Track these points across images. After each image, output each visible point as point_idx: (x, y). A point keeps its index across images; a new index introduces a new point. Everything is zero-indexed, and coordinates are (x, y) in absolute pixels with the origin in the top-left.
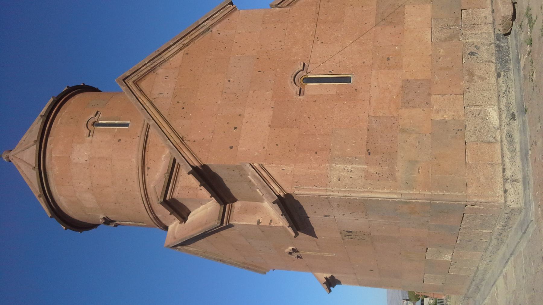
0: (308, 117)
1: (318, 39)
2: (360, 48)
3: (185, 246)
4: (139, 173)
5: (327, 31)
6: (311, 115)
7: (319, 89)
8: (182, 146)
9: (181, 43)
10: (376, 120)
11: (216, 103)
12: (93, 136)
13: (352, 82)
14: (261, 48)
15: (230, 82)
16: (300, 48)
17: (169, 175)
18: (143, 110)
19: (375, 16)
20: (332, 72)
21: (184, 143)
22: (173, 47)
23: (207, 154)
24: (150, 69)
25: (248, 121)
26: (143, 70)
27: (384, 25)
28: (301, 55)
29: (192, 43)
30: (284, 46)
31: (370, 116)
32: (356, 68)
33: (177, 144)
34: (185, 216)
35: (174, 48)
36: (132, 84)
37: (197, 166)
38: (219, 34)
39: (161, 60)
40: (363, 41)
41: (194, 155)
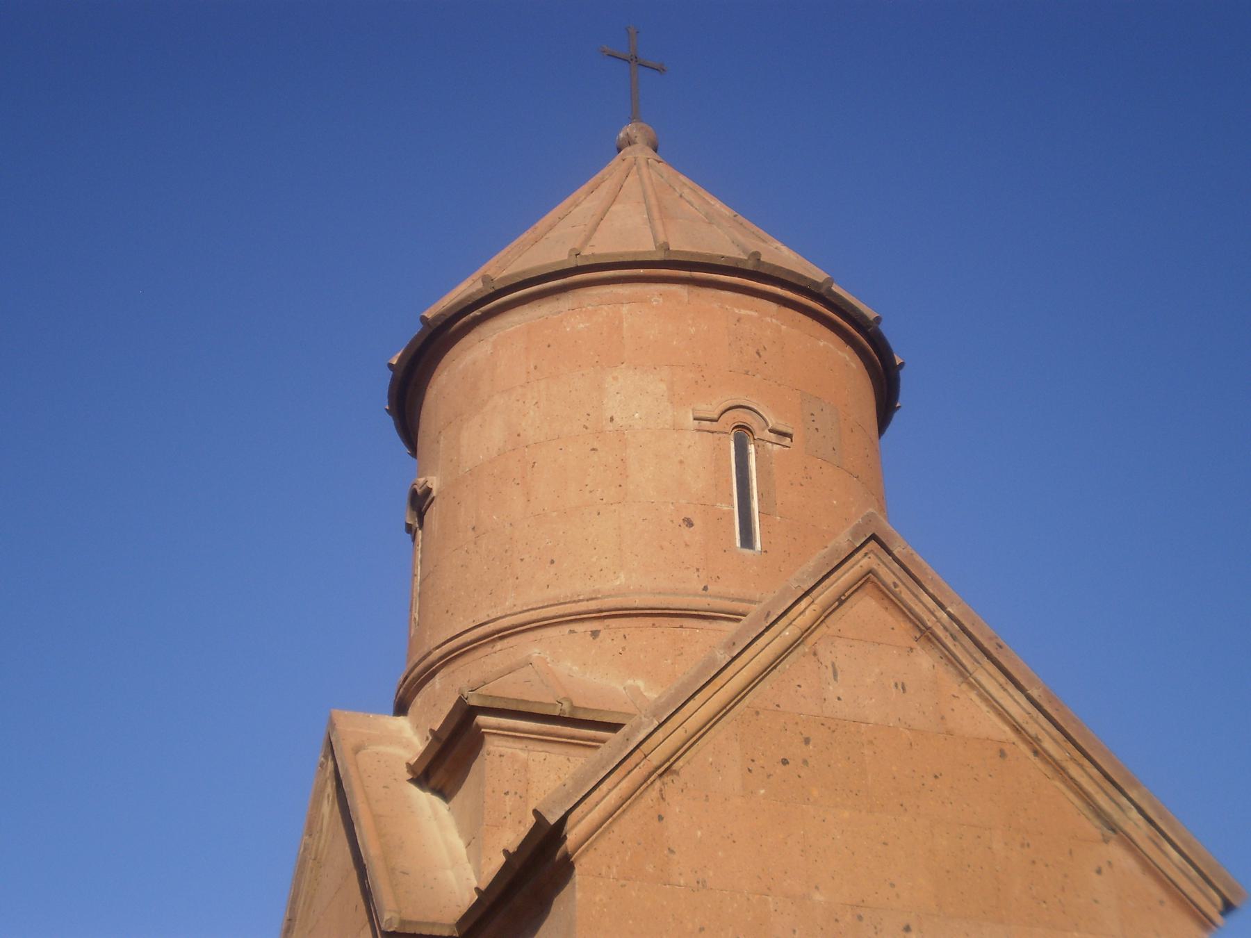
3: (334, 783)
4: (574, 602)
8: (637, 774)
9: (1044, 729)
11: (817, 888)
12: (698, 430)
17: (567, 715)
21: (652, 779)
23: (615, 870)
26: (921, 601)
29: (1048, 770)
33: (646, 756)
34: (433, 782)
35: (1018, 703)
36: (861, 566)
37: (565, 837)
39: (964, 661)
41: (605, 825)
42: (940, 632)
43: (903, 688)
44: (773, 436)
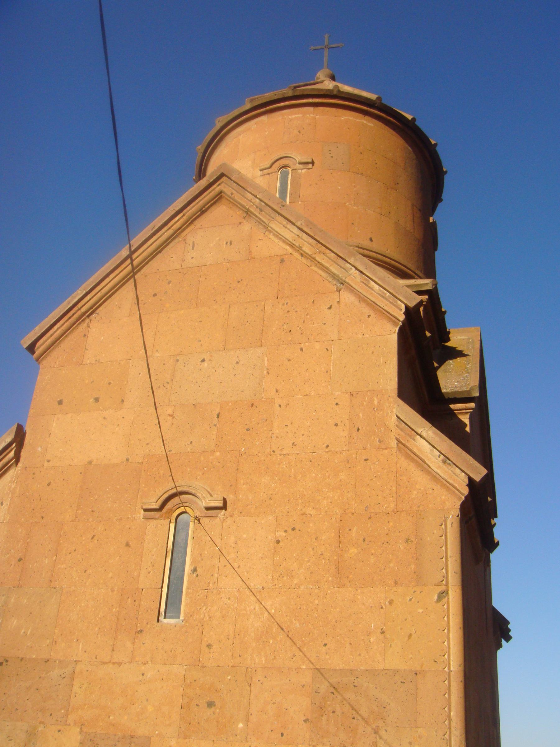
0: (94, 536)
1: (290, 530)
2: (252, 635)
5: (311, 549)
6: (98, 540)
7: (155, 550)
10: (64, 677)
11: (157, 351)
12: (263, 175)
13: (166, 621)
14: (280, 406)
15: (201, 363)
16: (271, 493)
18: (152, 230)
19: (347, 667)
20: (195, 575)
22: (295, 230)
24: (245, 208)
25: (106, 419)
27: (317, 692)
28: (250, 498)
29: (308, 262)
30: (280, 455)
31: (76, 664)
32: (196, 628)
38: (330, 308)
39: (264, 220)
40: (271, 642)
42: (252, 209)
43: (231, 244)
44: (301, 166)
